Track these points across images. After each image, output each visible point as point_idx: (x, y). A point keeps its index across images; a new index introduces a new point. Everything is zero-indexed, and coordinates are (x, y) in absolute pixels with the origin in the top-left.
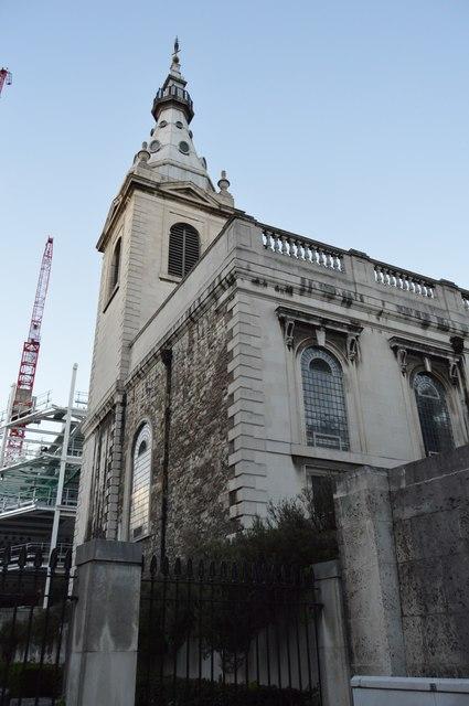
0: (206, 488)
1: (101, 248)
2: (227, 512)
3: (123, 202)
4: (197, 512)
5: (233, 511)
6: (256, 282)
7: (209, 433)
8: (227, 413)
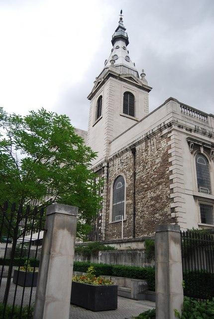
0: (157, 205)
1: (91, 97)
2: (170, 215)
3: (104, 81)
4: (154, 213)
5: (173, 215)
6: (179, 126)
7: (159, 184)
8: (169, 177)
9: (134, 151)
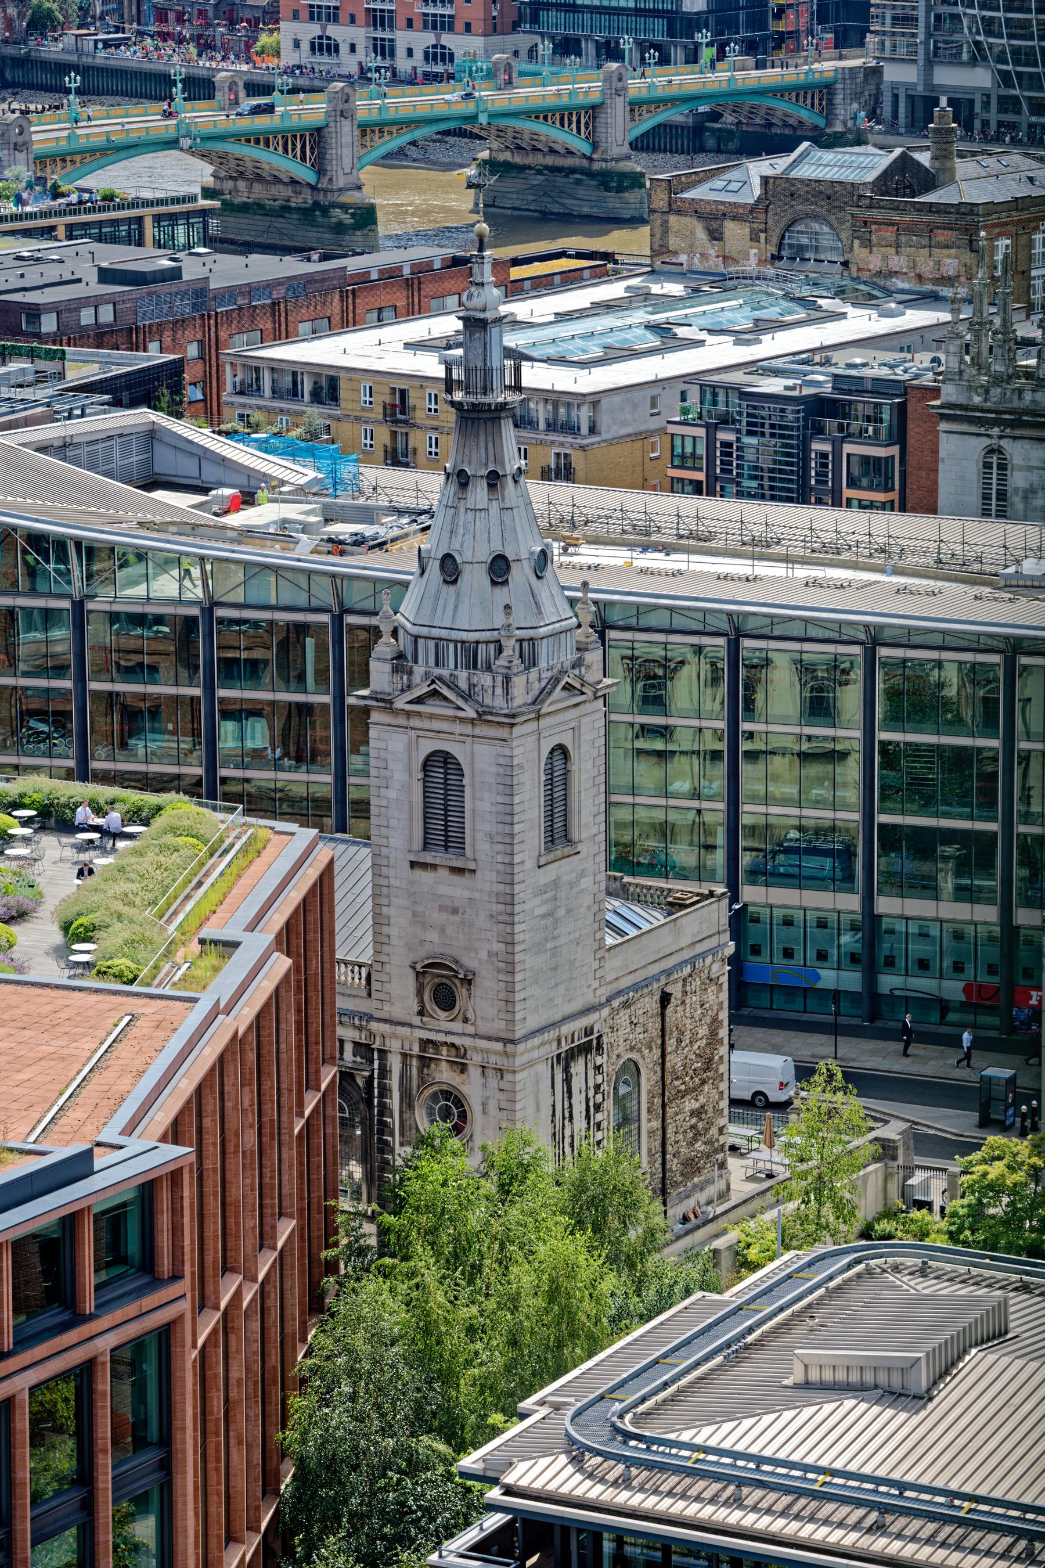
0: (700, 1125)
2: (717, 1140)
7: (703, 1082)
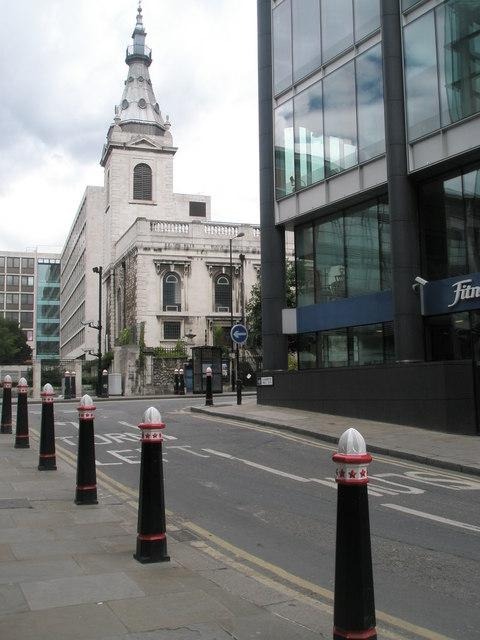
6: (146, 249)
9: (124, 266)
